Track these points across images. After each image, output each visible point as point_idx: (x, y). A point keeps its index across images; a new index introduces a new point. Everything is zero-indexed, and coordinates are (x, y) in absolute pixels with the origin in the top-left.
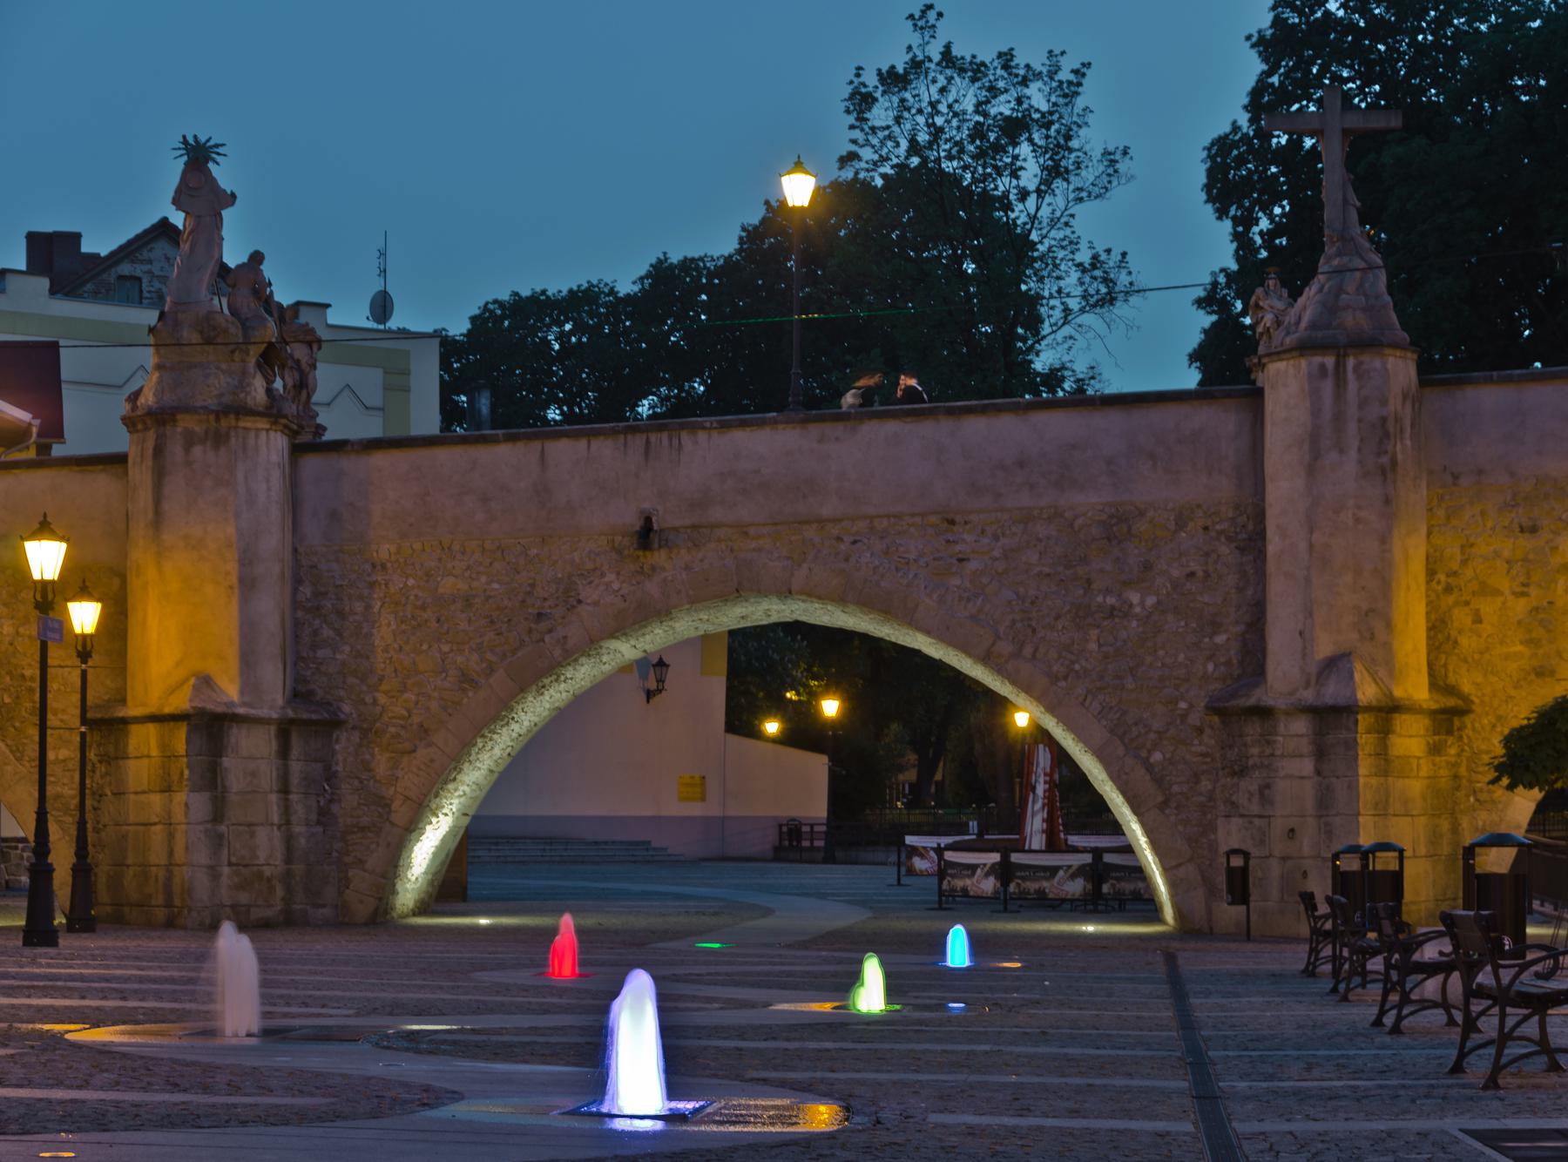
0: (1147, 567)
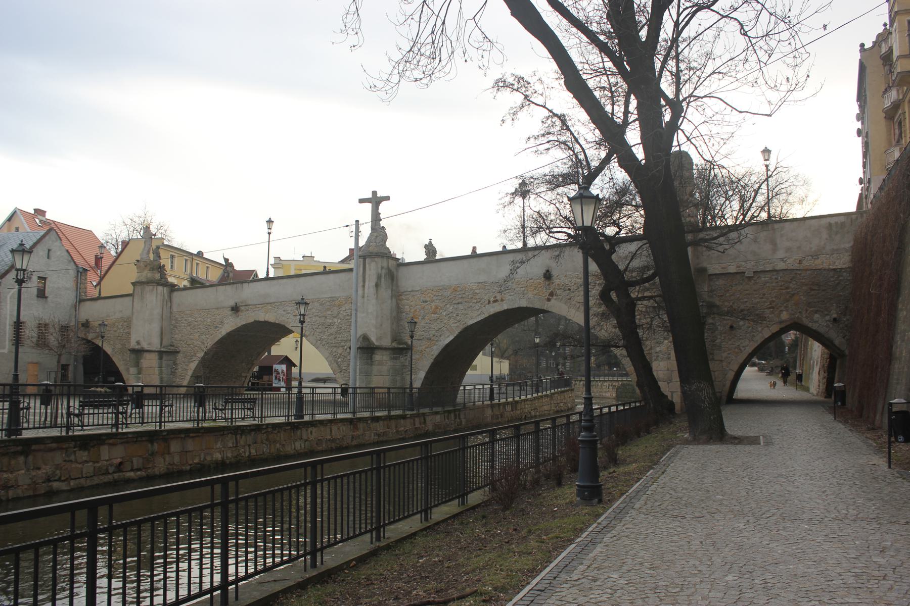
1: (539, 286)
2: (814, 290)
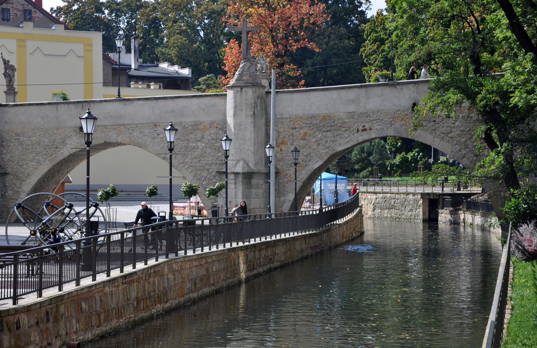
0: (203, 137)
1: (406, 117)
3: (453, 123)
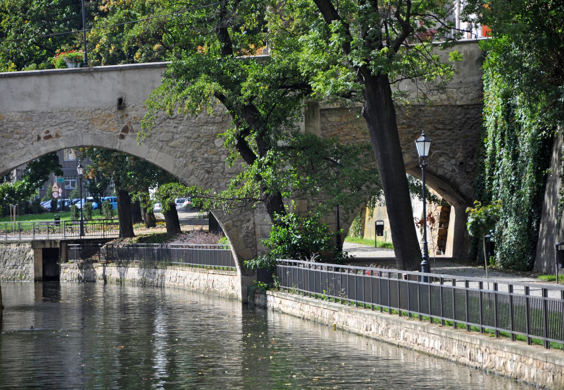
2: (439, 129)
3: (175, 127)
